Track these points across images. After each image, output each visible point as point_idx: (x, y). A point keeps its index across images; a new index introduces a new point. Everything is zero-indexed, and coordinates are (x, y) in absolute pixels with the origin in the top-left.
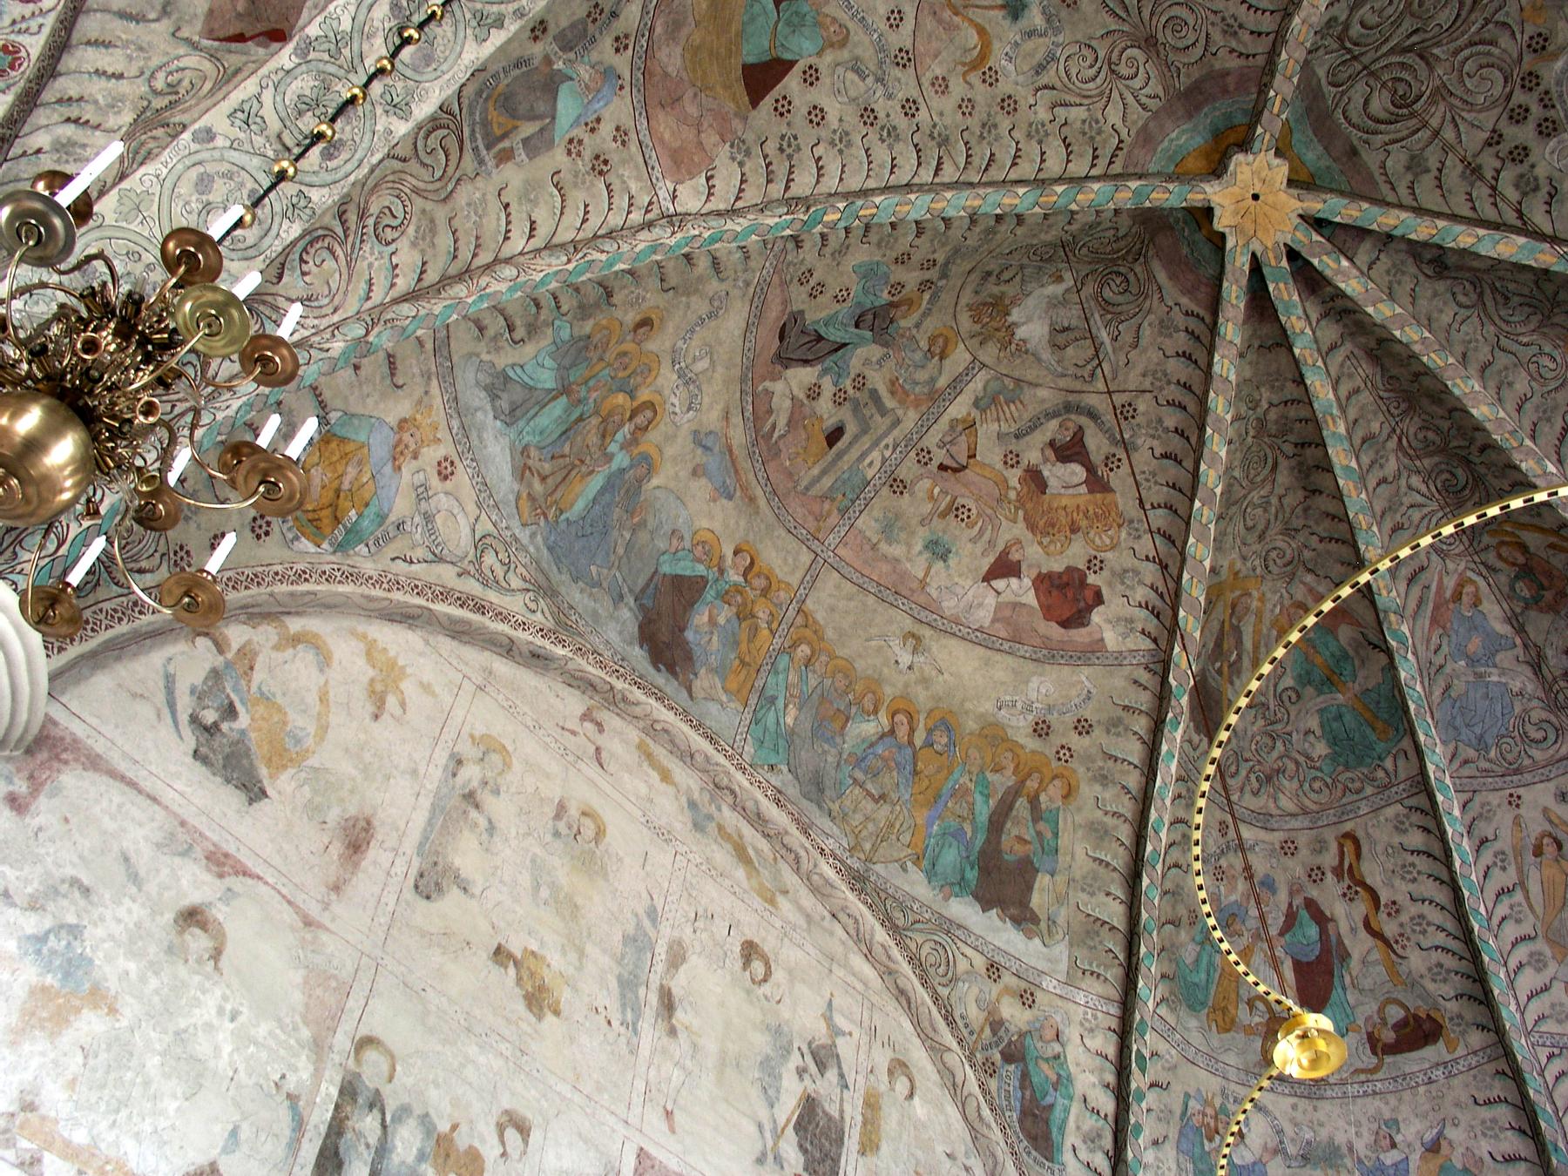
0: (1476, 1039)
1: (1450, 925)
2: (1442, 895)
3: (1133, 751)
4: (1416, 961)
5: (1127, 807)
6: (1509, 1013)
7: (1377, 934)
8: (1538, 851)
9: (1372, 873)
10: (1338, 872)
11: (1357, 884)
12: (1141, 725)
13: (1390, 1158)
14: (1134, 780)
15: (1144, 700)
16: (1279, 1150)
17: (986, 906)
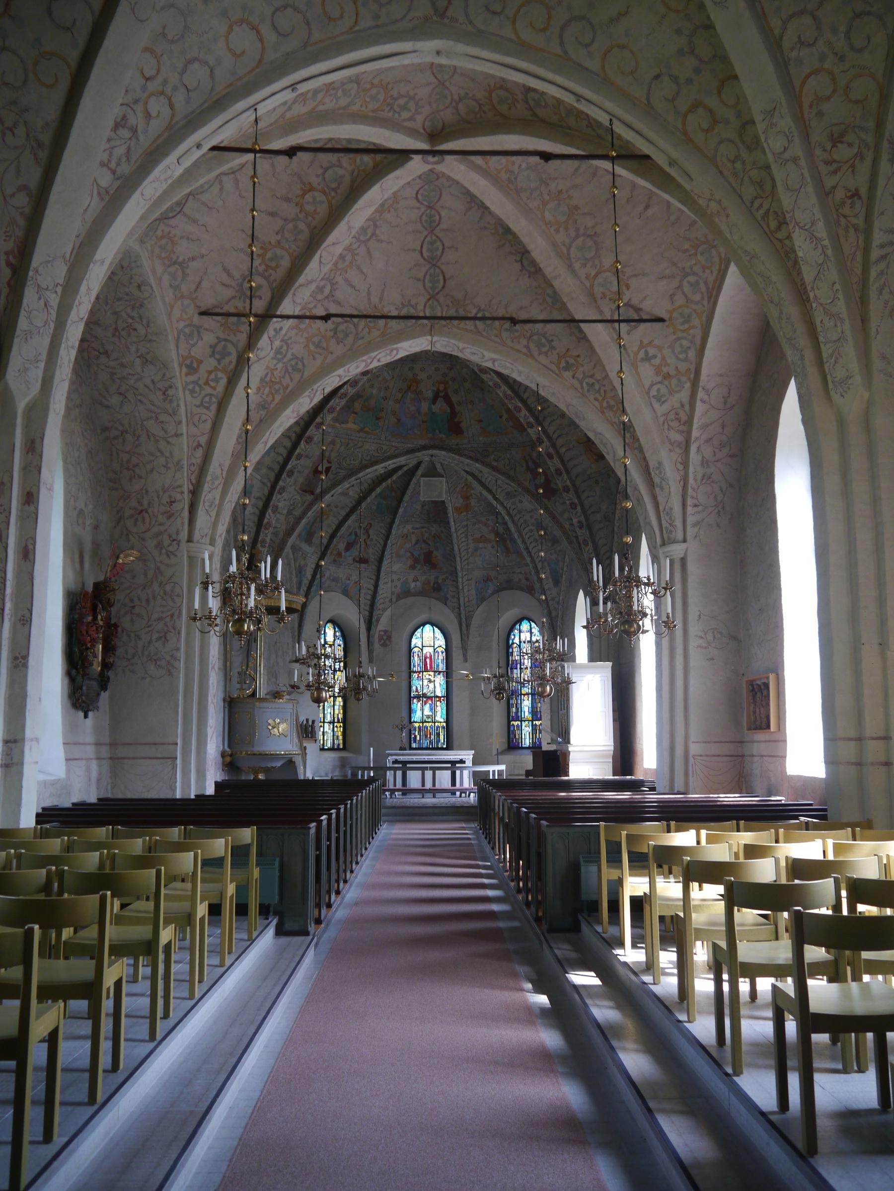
0: (374, 567)
1: (381, 548)
2: (382, 543)
3: (343, 513)
4: (371, 550)
5: (337, 522)
6: (383, 569)
7: (366, 543)
8: (403, 537)
9: (371, 532)
10: (364, 529)
11: (367, 531)
12: (348, 510)
13: (348, 582)
14: (340, 518)
15: (351, 505)
16: (329, 578)
17: (306, 542)
